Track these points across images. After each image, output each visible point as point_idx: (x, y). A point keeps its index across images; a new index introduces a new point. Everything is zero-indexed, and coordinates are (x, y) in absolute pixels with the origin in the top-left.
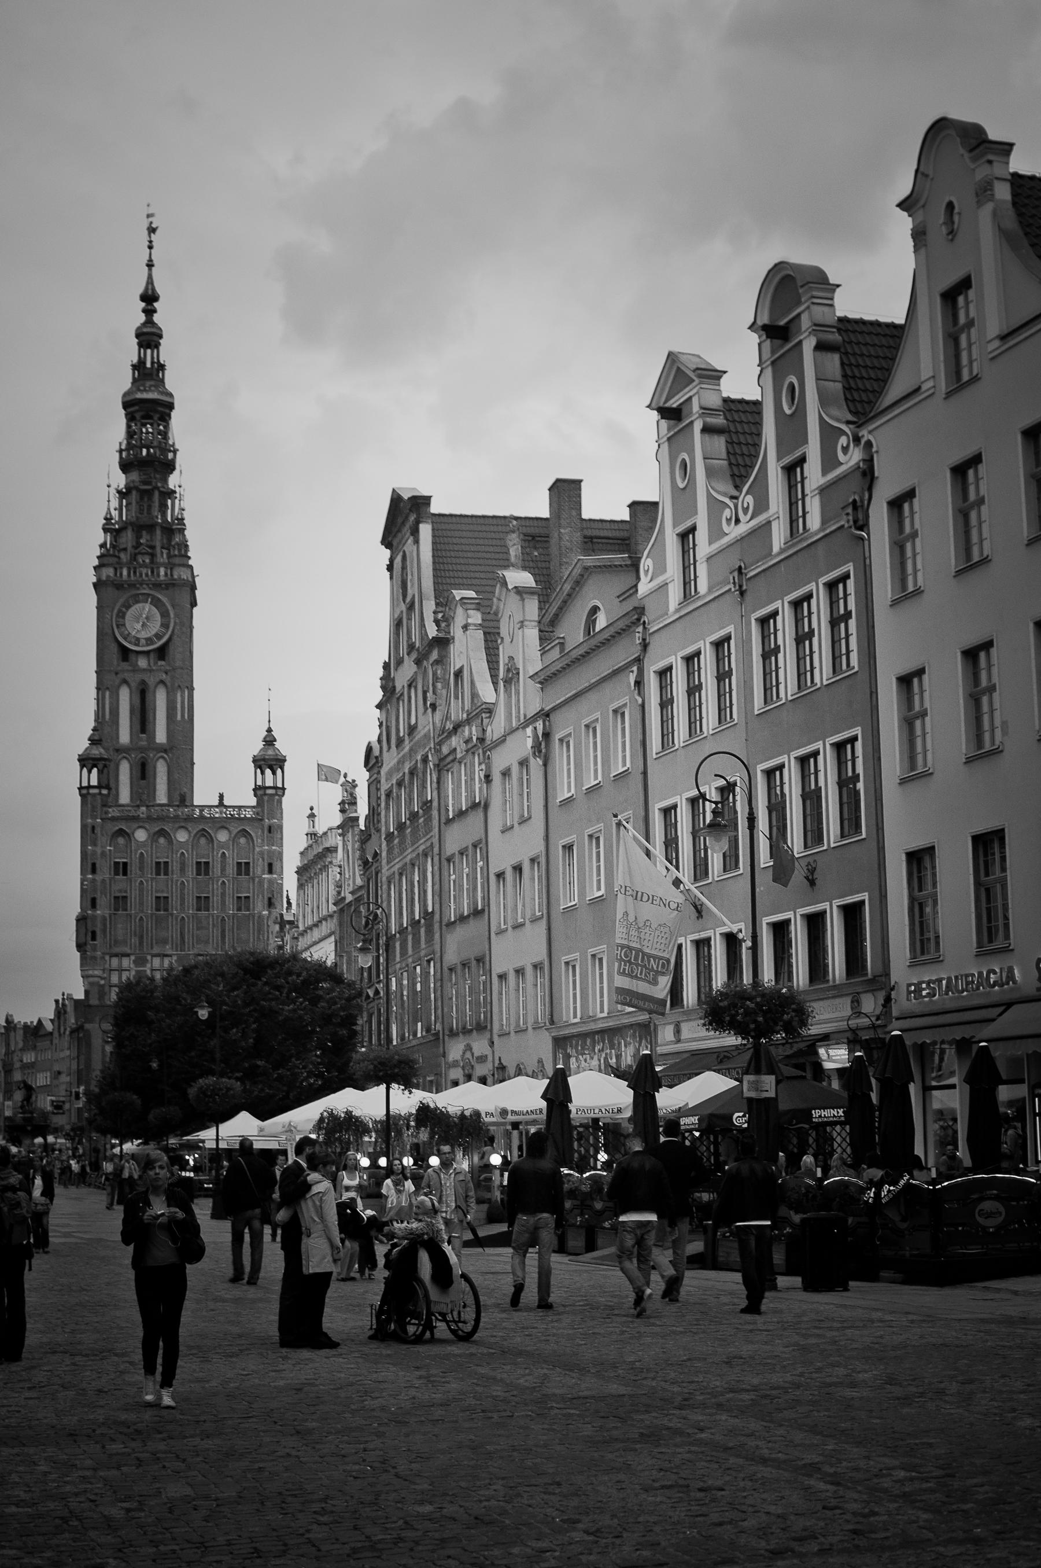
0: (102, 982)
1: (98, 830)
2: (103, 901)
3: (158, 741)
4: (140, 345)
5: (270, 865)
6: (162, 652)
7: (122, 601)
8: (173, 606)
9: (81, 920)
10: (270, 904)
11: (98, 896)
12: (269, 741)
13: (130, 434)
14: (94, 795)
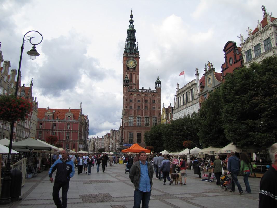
0: (128, 122)
1: (127, 93)
5: (159, 101)
6: (134, 68)
7: (128, 60)
8: (137, 61)
10: (159, 108)
12: (158, 79)
13: (128, 35)
14: (127, 87)
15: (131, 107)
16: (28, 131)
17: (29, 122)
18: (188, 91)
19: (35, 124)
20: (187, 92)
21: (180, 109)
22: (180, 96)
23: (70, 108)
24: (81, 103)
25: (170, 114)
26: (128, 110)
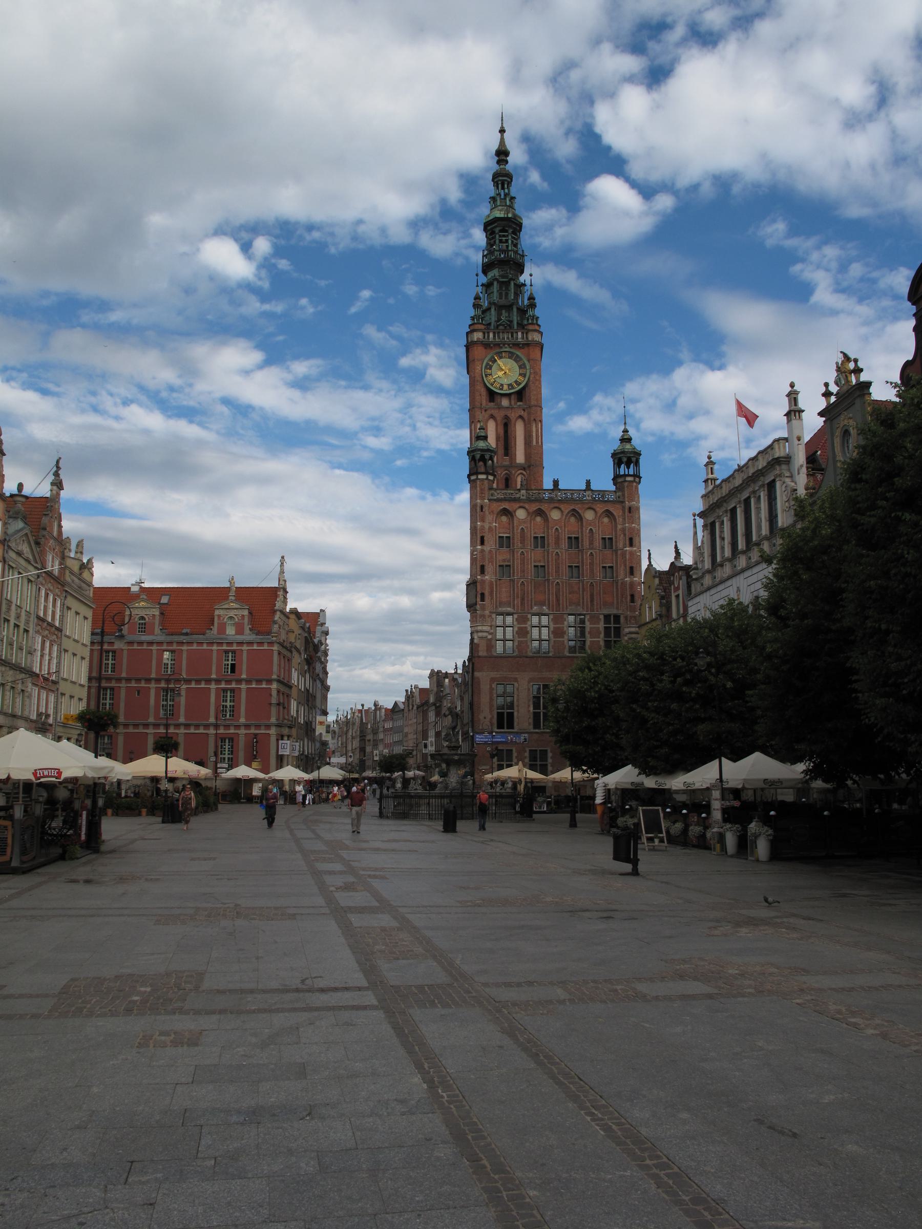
1: (486, 509)
2: (489, 568)
3: (518, 461)
4: (496, 184)
6: (520, 395)
7: (489, 357)
8: (529, 361)
9: (472, 585)
11: (486, 563)
14: (483, 480)
15: (505, 568)
16: (54, 688)
17: (55, 648)
18: (754, 492)
19: (83, 658)
20: (749, 498)
21: (720, 574)
22: (719, 517)
23: (231, 581)
24: (283, 557)
25: (677, 596)
26: (491, 583)
